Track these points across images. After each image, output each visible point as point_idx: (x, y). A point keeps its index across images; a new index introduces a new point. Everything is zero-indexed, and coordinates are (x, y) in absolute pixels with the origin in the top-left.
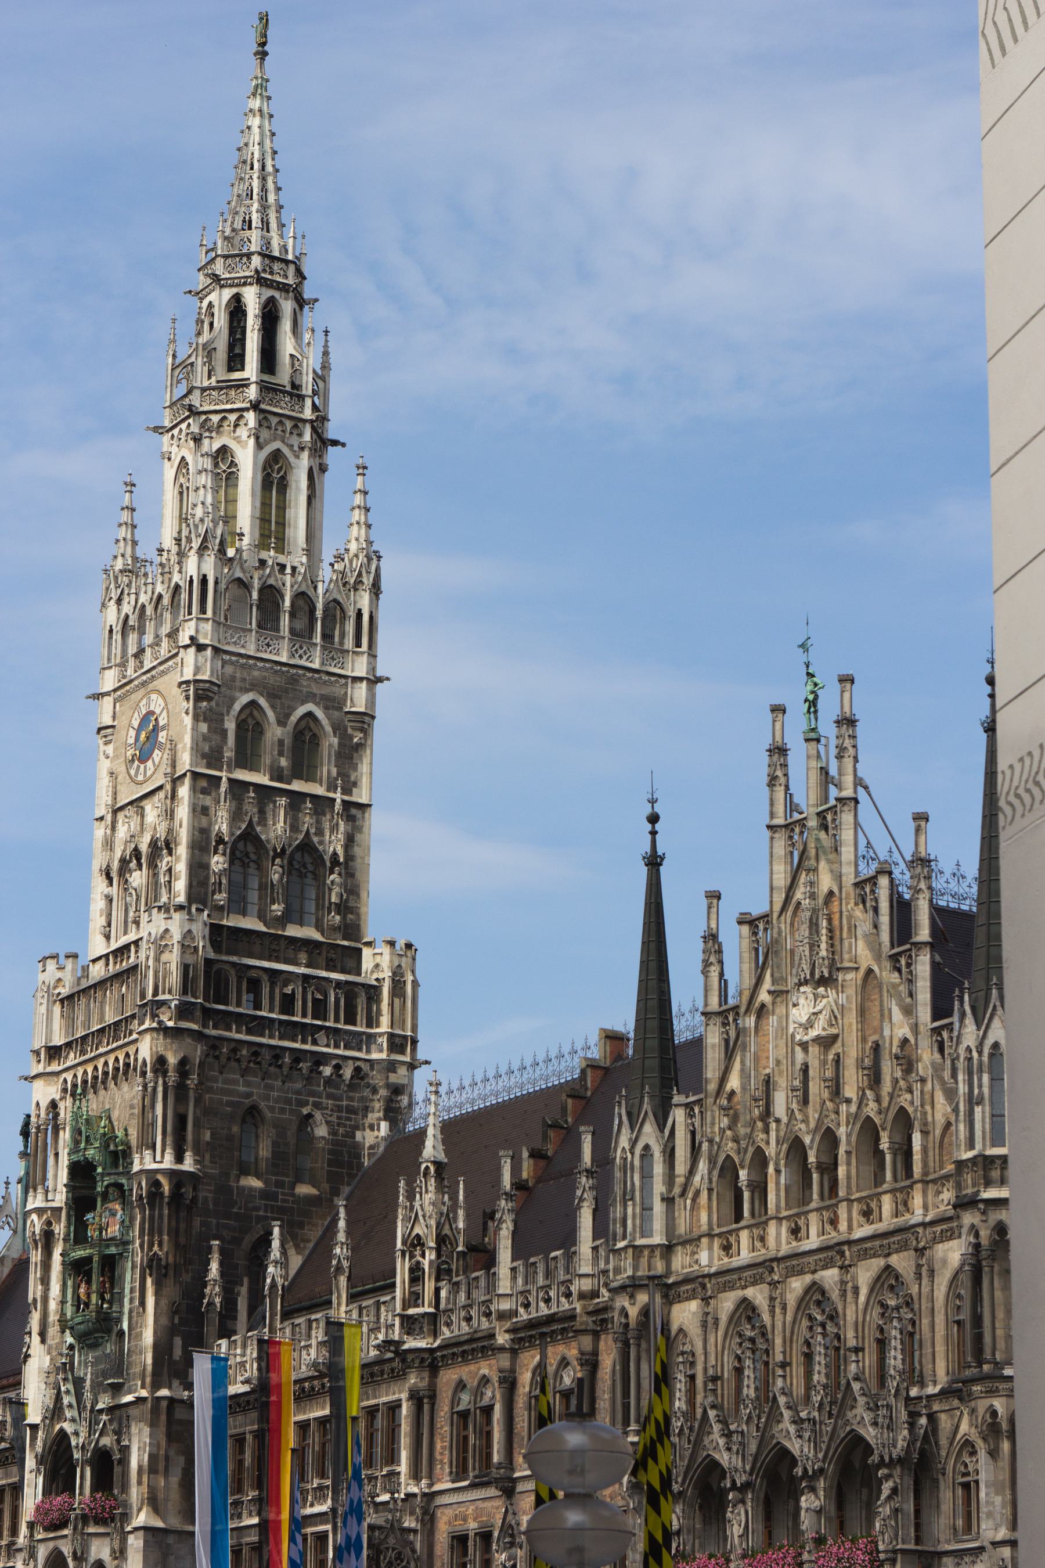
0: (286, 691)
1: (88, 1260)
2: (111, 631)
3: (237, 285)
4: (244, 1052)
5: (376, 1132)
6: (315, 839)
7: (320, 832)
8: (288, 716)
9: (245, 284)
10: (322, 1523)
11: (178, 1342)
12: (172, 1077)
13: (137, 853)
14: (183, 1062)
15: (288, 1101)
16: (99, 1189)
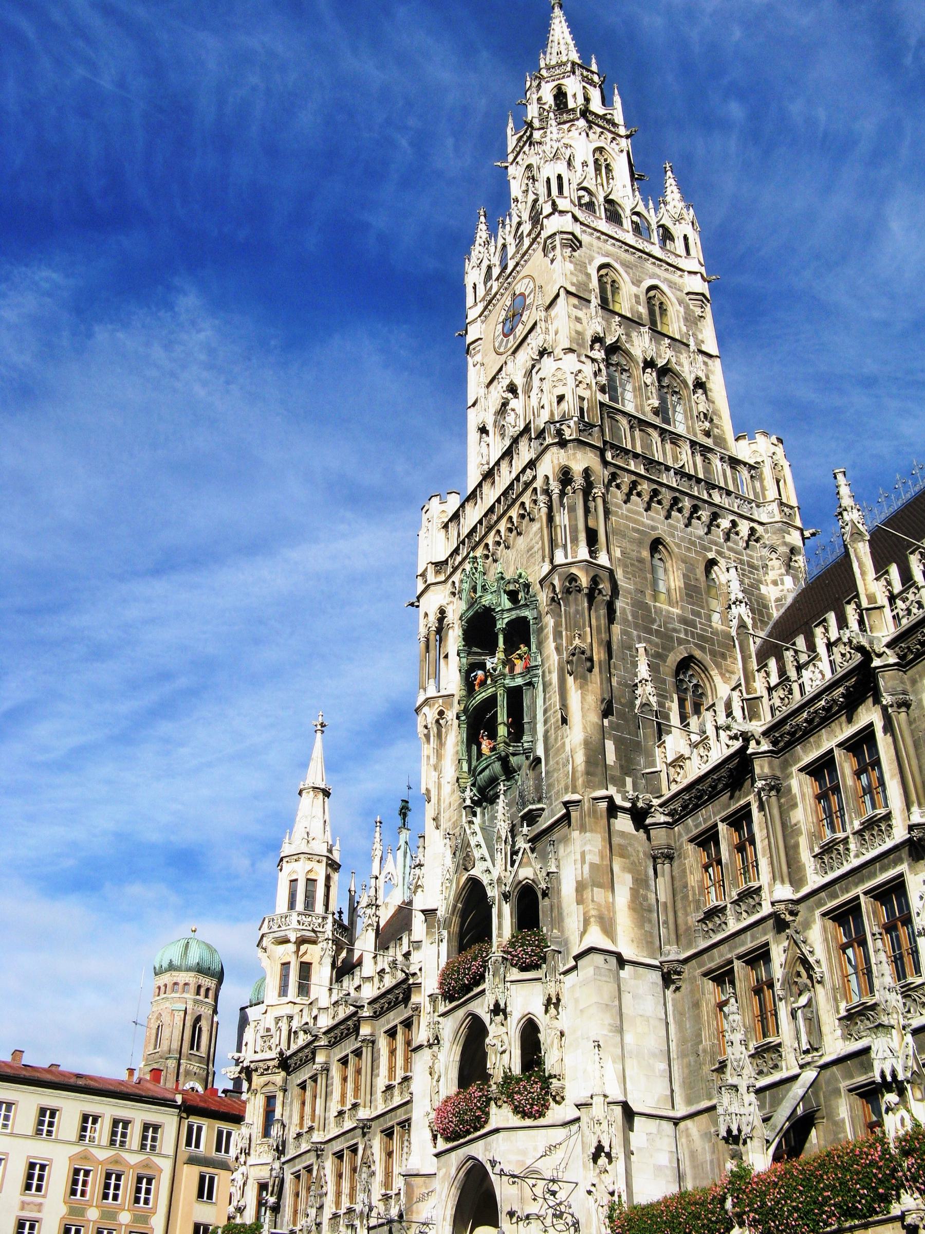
0: (636, 266)
1: (491, 702)
2: (475, 287)
3: (559, 79)
4: (645, 486)
5: (780, 587)
6: (678, 368)
7: (680, 365)
8: (641, 282)
9: (564, 77)
10: (884, 869)
11: (610, 746)
12: (579, 481)
13: (512, 389)
14: (587, 472)
15: (693, 543)
16: (498, 626)
